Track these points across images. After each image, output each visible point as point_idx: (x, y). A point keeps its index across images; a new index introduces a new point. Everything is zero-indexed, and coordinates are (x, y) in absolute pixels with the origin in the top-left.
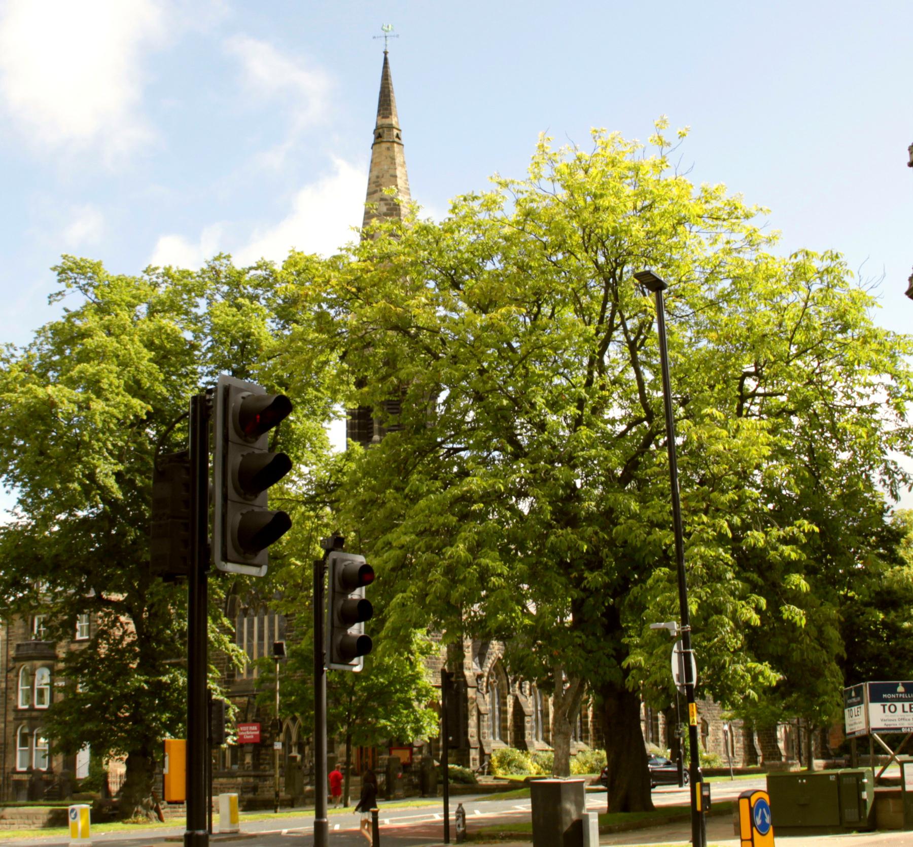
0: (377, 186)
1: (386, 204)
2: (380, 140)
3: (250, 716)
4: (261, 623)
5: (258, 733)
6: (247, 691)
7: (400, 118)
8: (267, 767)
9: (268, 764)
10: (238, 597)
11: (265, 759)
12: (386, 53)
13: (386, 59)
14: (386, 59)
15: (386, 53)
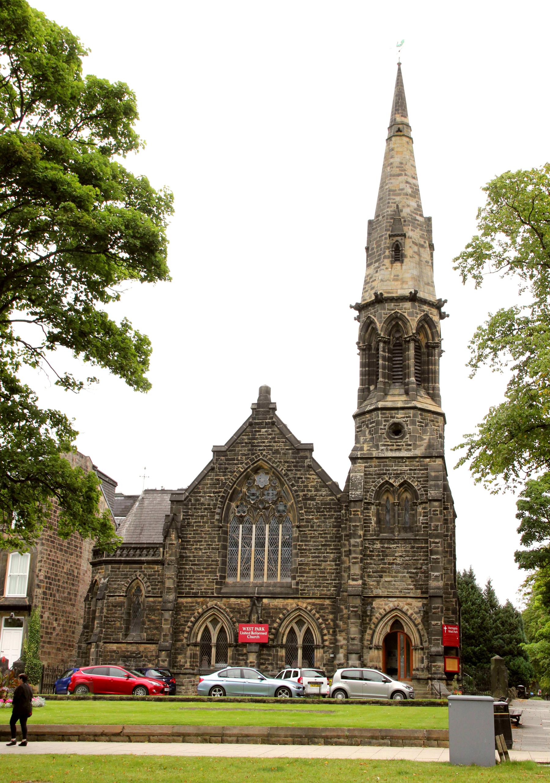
0: (402, 171)
1: (411, 187)
2: (399, 133)
3: (254, 617)
4: (261, 530)
5: (266, 633)
6: (246, 593)
7: (412, 119)
8: (270, 667)
9: (272, 664)
10: (233, 505)
11: (268, 660)
12: (399, 64)
13: (399, 69)
14: (399, 69)
15: (399, 64)
